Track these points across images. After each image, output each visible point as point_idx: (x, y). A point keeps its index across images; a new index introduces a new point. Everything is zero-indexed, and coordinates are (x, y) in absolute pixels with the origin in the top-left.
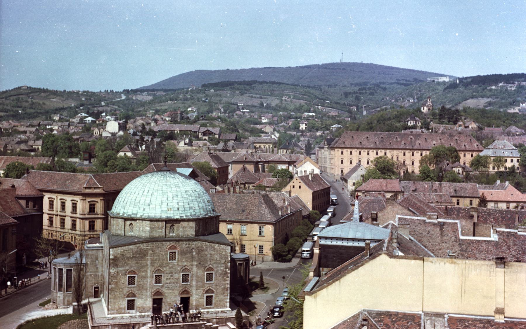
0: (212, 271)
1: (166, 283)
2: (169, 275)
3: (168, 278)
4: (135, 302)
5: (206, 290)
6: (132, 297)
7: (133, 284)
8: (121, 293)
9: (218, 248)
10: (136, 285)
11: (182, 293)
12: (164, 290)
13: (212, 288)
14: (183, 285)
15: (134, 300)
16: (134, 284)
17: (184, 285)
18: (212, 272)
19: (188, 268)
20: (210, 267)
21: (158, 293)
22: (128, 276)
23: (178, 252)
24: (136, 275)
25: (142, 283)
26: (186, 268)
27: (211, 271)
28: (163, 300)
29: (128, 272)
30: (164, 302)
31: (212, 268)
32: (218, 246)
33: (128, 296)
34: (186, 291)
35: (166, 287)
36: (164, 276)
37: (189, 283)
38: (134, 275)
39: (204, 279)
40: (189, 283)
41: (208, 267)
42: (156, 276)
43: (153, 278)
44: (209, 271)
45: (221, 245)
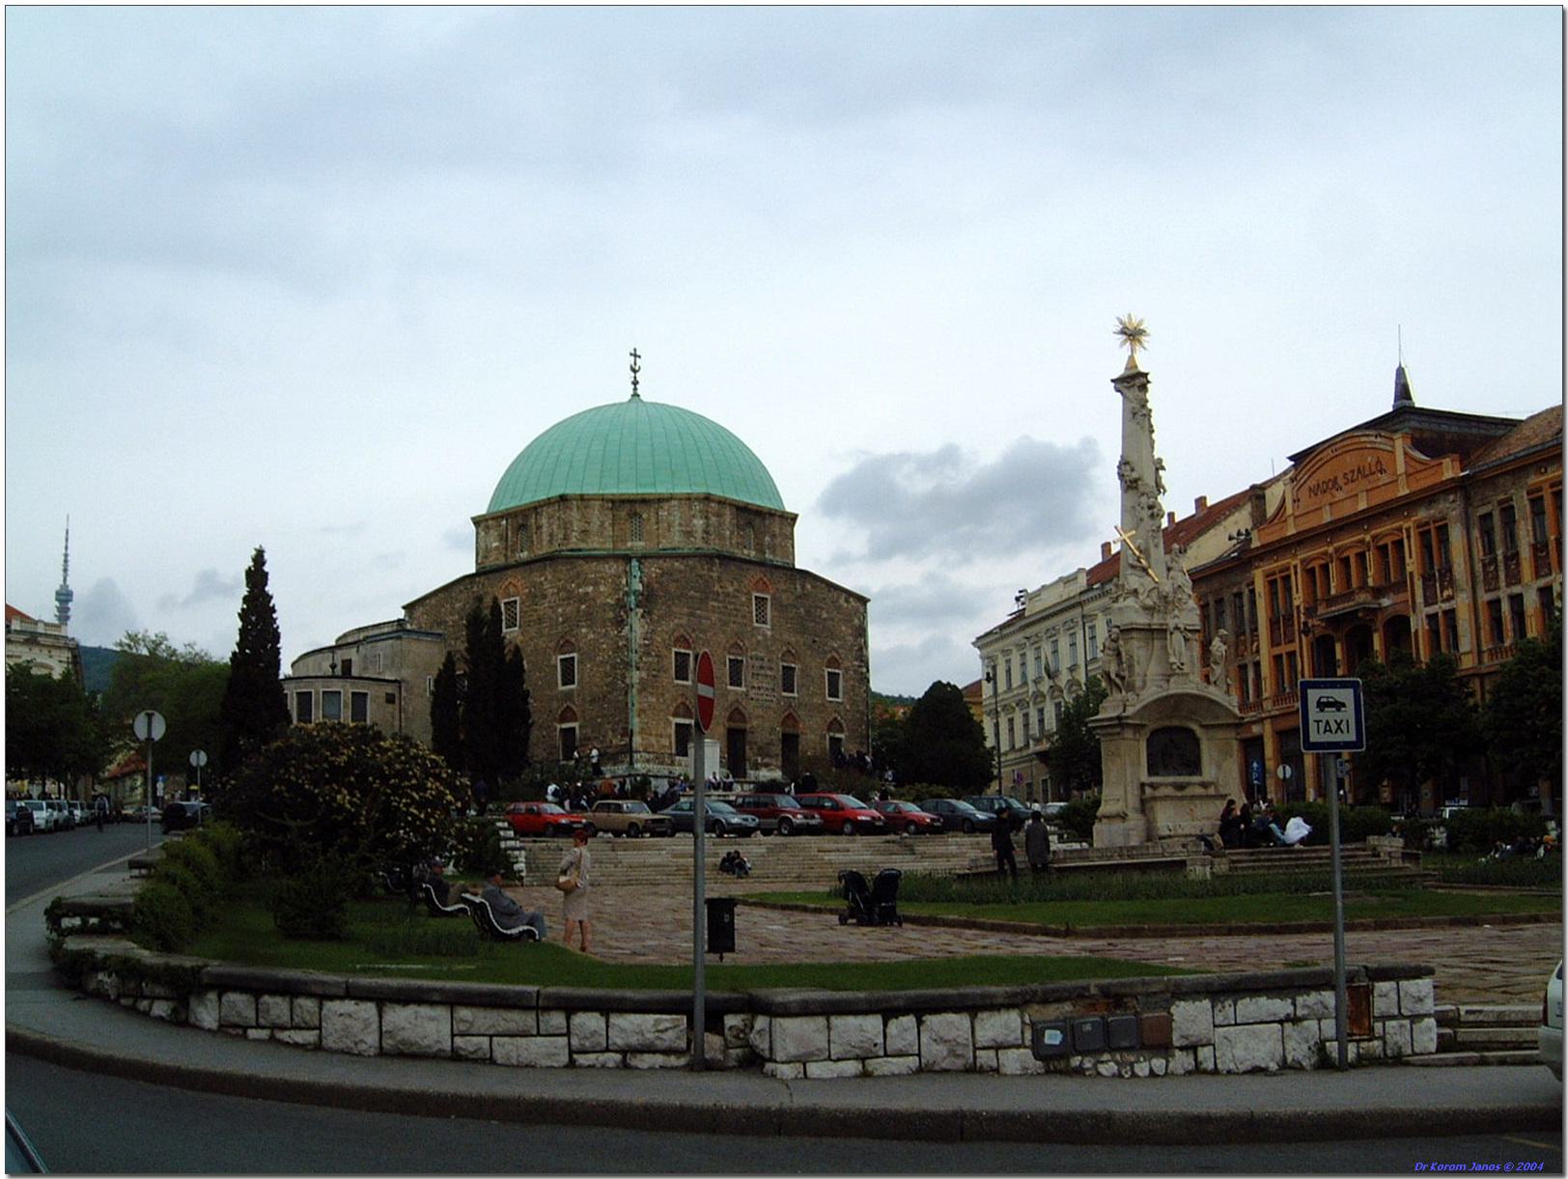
1: (753, 687)
2: (758, 664)
6: (684, 717)
7: (683, 679)
9: (845, 605)
12: (749, 708)
18: (837, 671)
20: (833, 657)
22: (674, 650)
26: (789, 651)
28: (749, 737)
30: (750, 743)
32: (847, 601)
33: (676, 715)
34: (790, 719)
40: (795, 695)
41: (829, 656)
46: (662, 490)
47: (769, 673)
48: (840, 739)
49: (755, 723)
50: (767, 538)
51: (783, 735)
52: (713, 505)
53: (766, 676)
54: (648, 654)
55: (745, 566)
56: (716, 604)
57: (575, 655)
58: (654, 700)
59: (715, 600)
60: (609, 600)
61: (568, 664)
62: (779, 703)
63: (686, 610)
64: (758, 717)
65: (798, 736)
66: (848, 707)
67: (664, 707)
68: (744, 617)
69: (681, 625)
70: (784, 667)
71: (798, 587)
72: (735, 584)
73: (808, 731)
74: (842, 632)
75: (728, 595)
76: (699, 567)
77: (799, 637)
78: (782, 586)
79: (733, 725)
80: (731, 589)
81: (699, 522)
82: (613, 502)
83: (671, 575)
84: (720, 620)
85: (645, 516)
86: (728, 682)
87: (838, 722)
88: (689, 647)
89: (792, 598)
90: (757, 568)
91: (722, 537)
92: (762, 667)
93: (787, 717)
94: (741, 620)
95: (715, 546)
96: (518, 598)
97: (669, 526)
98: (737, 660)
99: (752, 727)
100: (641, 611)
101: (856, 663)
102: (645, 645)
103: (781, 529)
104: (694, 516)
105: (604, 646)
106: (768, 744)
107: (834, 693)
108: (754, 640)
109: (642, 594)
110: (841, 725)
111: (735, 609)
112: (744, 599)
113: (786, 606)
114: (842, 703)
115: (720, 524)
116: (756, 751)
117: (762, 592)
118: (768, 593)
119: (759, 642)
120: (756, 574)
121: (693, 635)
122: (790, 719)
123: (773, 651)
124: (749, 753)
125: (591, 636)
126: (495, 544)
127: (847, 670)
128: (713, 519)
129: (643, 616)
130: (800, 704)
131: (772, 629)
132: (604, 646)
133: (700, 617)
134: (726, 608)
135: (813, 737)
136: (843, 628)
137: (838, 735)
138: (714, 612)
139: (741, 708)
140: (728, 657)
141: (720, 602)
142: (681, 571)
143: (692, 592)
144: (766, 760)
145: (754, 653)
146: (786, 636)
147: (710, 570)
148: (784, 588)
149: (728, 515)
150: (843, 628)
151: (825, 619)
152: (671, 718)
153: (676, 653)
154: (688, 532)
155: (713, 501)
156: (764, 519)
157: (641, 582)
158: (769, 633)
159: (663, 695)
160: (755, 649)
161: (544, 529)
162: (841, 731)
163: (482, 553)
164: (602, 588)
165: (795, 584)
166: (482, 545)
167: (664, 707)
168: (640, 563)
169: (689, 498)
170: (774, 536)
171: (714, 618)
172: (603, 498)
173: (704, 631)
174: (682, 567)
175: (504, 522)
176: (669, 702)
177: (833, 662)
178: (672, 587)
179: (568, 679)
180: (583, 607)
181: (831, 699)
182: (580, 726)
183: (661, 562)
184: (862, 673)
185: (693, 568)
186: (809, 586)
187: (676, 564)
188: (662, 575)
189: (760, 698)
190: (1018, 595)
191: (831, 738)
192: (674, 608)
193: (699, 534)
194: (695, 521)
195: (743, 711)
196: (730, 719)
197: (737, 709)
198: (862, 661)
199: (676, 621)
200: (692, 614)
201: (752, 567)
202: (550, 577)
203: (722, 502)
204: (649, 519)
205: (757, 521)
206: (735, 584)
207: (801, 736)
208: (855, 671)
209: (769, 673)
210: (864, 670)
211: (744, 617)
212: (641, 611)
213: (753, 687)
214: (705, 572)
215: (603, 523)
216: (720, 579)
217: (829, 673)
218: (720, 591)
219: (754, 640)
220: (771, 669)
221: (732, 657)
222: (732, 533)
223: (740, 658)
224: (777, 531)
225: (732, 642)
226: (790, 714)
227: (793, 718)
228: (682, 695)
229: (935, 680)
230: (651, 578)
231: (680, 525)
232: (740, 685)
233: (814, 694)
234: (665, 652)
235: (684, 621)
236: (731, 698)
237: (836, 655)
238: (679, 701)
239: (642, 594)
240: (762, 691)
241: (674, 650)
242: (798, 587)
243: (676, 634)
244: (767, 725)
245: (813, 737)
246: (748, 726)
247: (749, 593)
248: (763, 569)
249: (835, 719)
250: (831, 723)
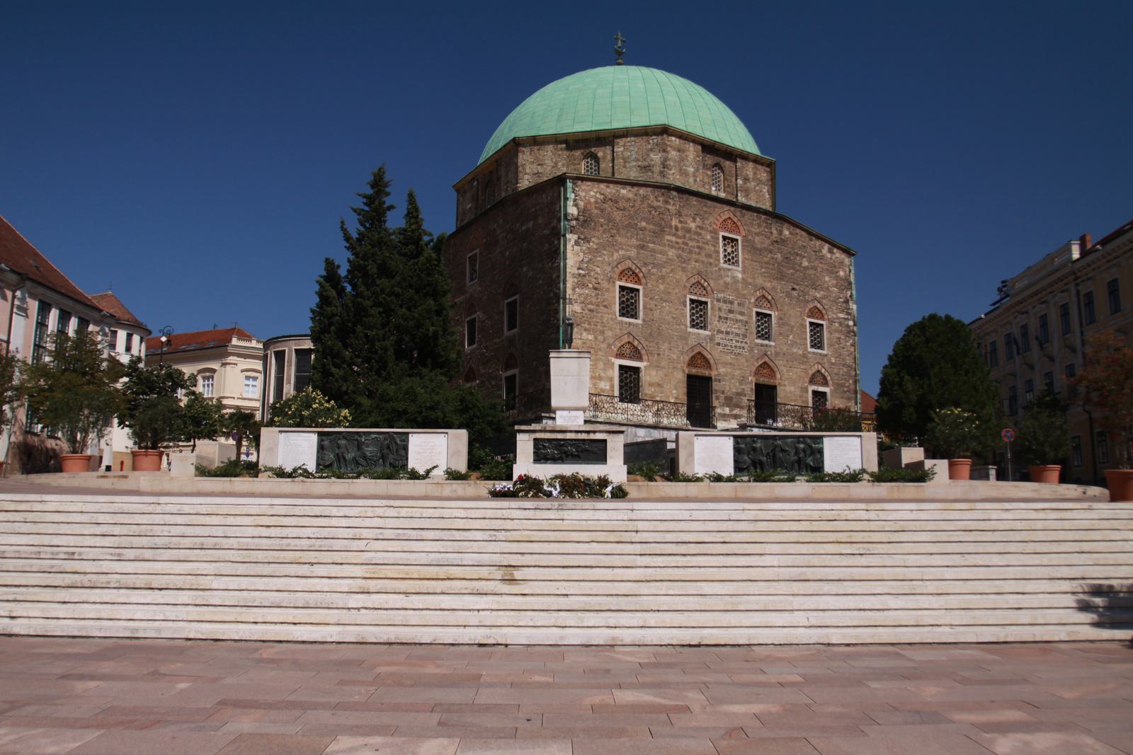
0: (822, 318)
1: (720, 332)
2: (725, 306)
3: (723, 315)
4: (642, 374)
5: (811, 372)
6: (631, 358)
7: (632, 316)
8: (600, 338)
9: (829, 256)
10: (639, 321)
11: (757, 372)
12: (713, 354)
13: (823, 371)
14: (757, 344)
15: (637, 370)
16: (635, 316)
17: (762, 345)
19: (767, 295)
20: (816, 307)
21: (698, 359)
22: (619, 283)
23: (743, 242)
24: (640, 287)
25: (657, 314)
26: (764, 296)
27: (817, 318)
28: (716, 386)
29: (617, 271)
30: (716, 390)
31: (819, 310)
32: (830, 251)
33: (620, 355)
34: (766, 367)
35: (719, 344)
36: (712, 308)
37: (772, 343)
38: (636, 287)
39: (806, 339)
40: (772, 343)
41: (811, 305)
42: (692, 301)
43: (685, 306)
44: (813, 317)
45: (835, 250)
46: (617, 125)
47: (740, 317)
48: (824, 394)
49: (722, 370)
50: (740, 182)
51: (757, 385)
52: (673, 138)
53: (737, 320)
54: (584, 286)
55: (709, 203)
56: (674, 239)
57: (517, 297)
58: (590, 337)
59: (674, 235)
60: (546, 232)
61: (512, 306)
62: (751, 350)
63: (634, 241)
64: (726, 364)
65: (774, 388)
66: (833, 361)
67: (603, 346)
68: (709, 256)
69: (629, 258)
70: (758, 314)
71: (774, 231)
72: (698, 219)
73: (786, 383)
74: (826, 282)
75: (689, 231)
76: (652, 198)
77: (775, 283)
78: (755, 229)
79: (694, 371)
80: (693, 226)
81: (656, 157)
82: (566, 142)
83: (617, 202)
84: (679, 256)
85: (600, 154)
86: (689, 324)
87: (823, 375)
88: (638, 282)
89: (768, 242)
90: (726, 208)
91: (683, 173)
92: (731, 311)
93: (761, 366)
94: (704, 259)
95: (674, 178)
96: (478, 250)
97: (625, 162)
98: (702, 303)
99: (719, 374)
100: (575, 237)
101: (842, 315)
102: (580, 275)
103: (755, 174)
104: (651, 150)
105: (541, 282)
106: (738, 394)
107: (817, 344)
108: (721, 282)
109: (577, 219)
110: (825, 378)
111: (698, 247)
112: (709, 237)
113: (760, 250)
114: (826, 355)
115: (682, 160)
116: (722, 400)
117: (730, 232)
118: (739, 233)
119: (726, 284)
120: (726, 212)
121: (643, 269)
122: (766, 367)
123: (744, 296)
124: (715, 403)
125: (530, 274)
126: (469, 206)
127: (831, 321)
128: (673, 154)
129: (577, 243)
130: (777, 354)
131: (744, 272)
132: (541, 282)
133: (653, 251)
134: (687, 245)
135: (792, 389)
136: (827, 279)
137: (821, 389)
138: (672, 247)
139: (705, 353)
140: (689, 297)
141: (677, 236)
142: (629, 199)
143: (644, 224)
144: (736, 411)
145: (721, 295)
146: (760, 281)
147: (666, 202)
148: (758, 231)
149: (692, 151)
150: (827, 279)
151: (806, 268)
152: (613, 360)
153: (621, 287)
154: (645, 167)
155: (672, 135)
156: (735, 162)
157: (576, 205)
158: (740, 276)
159: (602, 332)
160: (723, 291)
161: (503, 179)
162: (825, 383)
163: (460, 214)
164: (540, 221)
165: (771, 228)
166: (461, 209)
167: (603, 346)
168: (574, 184)
169: (645, 132)
170: (746, 179)
171: (672, 253)
172: (556, 140)
173: (655, 266)
174: (631, 195)
175: (475, 183)
176: (611, 341)
177: (815, 312)
178: (617, 216)
179: (512, 326)
180: (525, 244)
181: (813, 350)
182: (520, 372)
183: (602, 186)
184: (848, 326)
185: (644, 198)
186: (786, 232)
187: (623, 192)
188: (604, 201)
189: (727, 343)
190: (1000, 285)
191: (815, 393)
192: (619, 239)
193: (657, 169)
194: (652, 156)
195: (709, 357)
196: (692, 363)
197: (699, 353)
198: (850, 314)
199: (620, 252)
200: (642, 247)
201: (718, 205)
202: (501, 223)
203: (685, 137)
204: (604, 157)
205: (727, 164)
206: (698, 219)
207: (779, 389)
208: (841, 324)
209: (740, 317)
210: (851, 323)
211: (709, 256)
212: (575, 237)
213: (720, 332)
214: (660, 204)
215: (556, 164)
216: (679, 214)
217: (811, 324)
218: (679, 225)
219: (721, 282)
220: (742, 314)
221: (693, 297)
222: (697, 170)
223: (703, 299)
224: (750, 174)
225: (693, 280)
226: (765, 363)
227: (770, 367)
228: (629, 333)
229: (933, 312)
230: (590, 202)
231: (637, 160)
232: (704, 328)
233: (794, 344)
234: (605, 284)
235: (633, 253)
236: (692, 342)
237: (819, 306)
238: (626, 339)
239: (576, 219)
240: (731, 337)
241: (619, 283)
242: (774, 231)
243: (621, 268)
244: (738, 372)
245: (792, 389)
246: (713, 374)
247: (715, 232)
248: (732, 209)
249: (819, 371)
250: (814, 375)
